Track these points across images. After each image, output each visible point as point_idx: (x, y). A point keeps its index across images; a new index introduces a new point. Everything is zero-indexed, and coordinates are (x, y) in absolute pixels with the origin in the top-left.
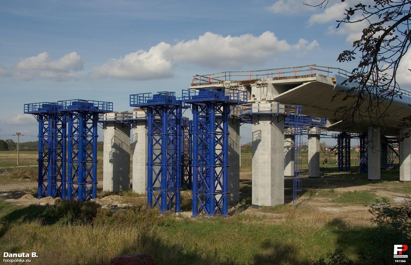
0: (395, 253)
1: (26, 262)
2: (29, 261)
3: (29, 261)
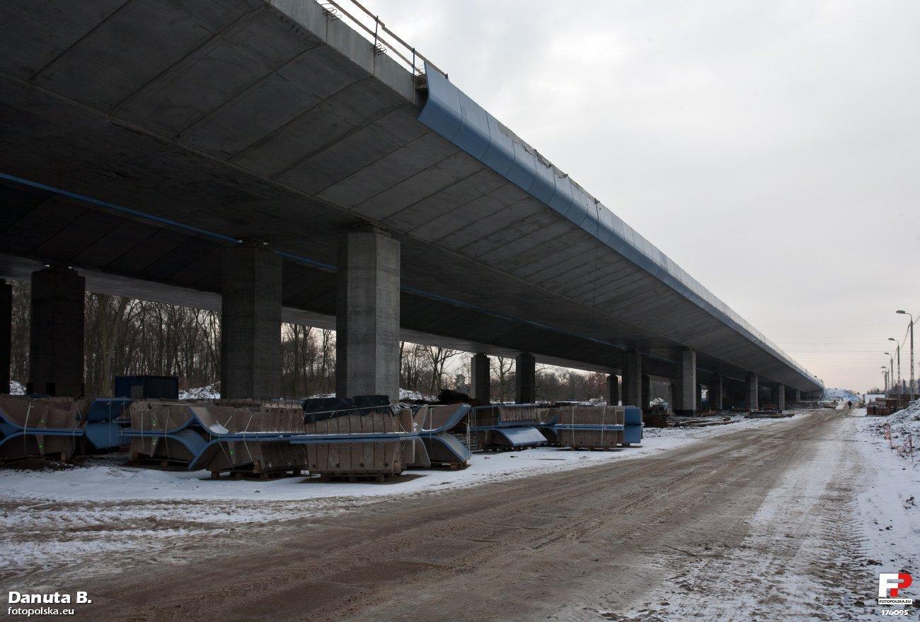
0: (883, 592)
1: (63, 614)
2: (71, 612)
3: (71, 612)
